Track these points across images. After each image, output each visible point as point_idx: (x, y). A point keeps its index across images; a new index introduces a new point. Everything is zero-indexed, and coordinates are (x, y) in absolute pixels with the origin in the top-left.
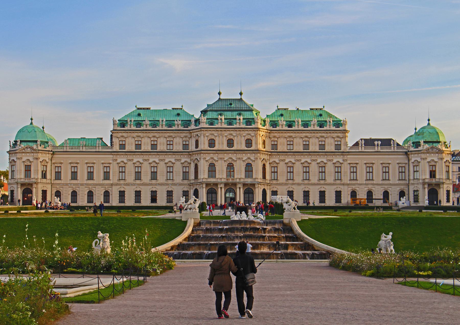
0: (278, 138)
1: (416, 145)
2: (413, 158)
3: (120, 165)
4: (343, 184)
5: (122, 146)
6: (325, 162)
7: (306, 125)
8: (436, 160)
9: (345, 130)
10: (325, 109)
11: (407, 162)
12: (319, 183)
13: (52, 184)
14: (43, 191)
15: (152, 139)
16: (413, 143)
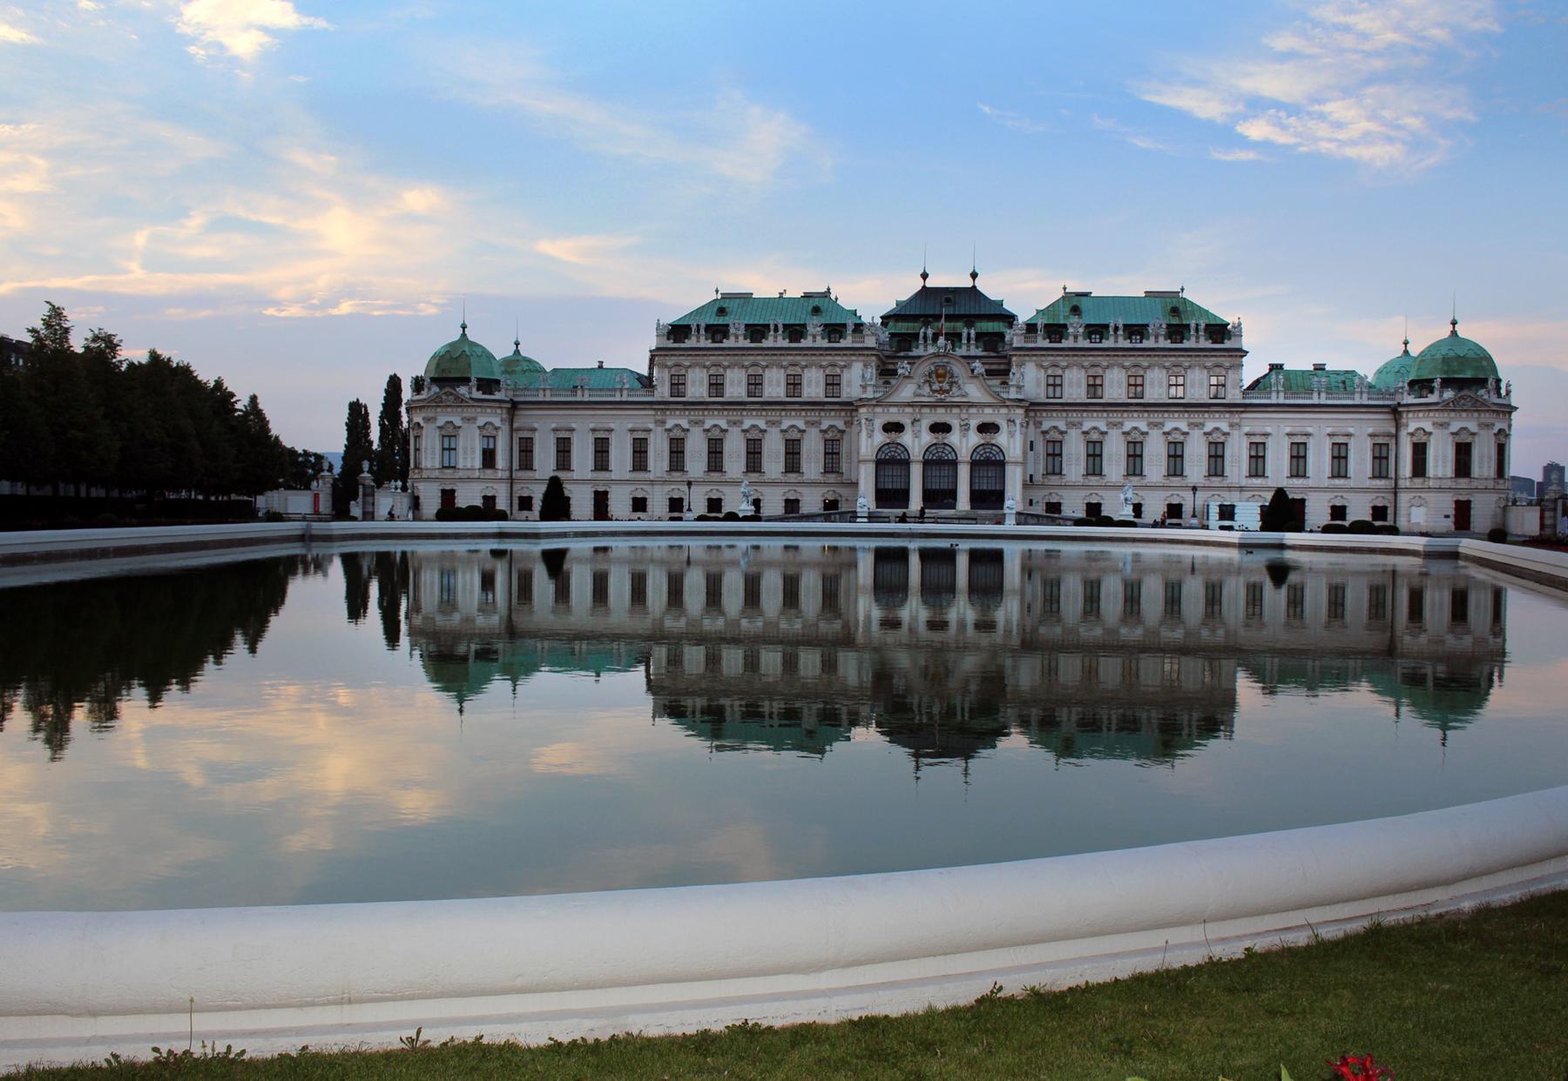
0: (1064, 369)
1: (1421, 389)
2: (1413, 423)
3: (672, 435)
4: (1230, 488)
5: (677, 386)
6: (1186, 429)
7: (1136, 331)
8: (1473, 427)
9: (1240, 350)
10: (1185, 295)
11: (1393, 431)
12: (1167, 483)
13: (511, 480)
14: (485, 498)
15: (750, 371)
16: (1412, 384)
